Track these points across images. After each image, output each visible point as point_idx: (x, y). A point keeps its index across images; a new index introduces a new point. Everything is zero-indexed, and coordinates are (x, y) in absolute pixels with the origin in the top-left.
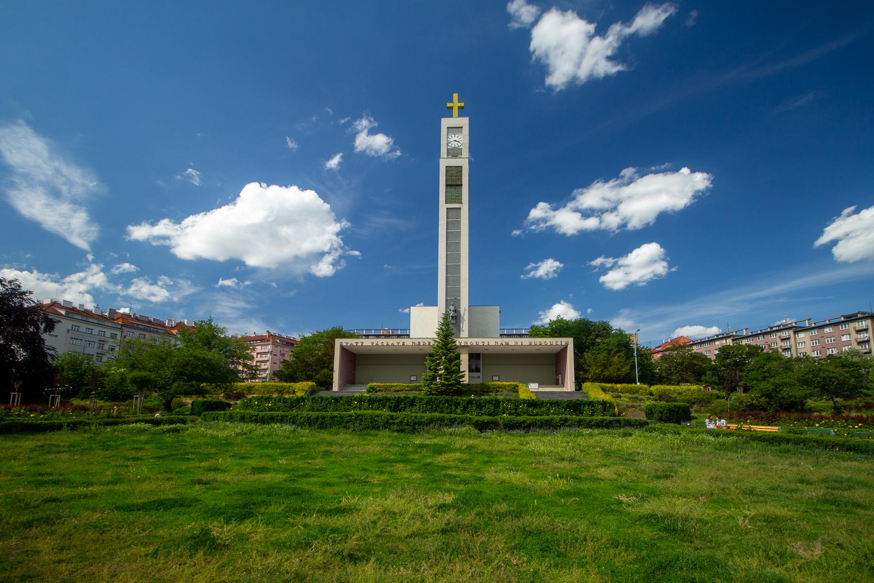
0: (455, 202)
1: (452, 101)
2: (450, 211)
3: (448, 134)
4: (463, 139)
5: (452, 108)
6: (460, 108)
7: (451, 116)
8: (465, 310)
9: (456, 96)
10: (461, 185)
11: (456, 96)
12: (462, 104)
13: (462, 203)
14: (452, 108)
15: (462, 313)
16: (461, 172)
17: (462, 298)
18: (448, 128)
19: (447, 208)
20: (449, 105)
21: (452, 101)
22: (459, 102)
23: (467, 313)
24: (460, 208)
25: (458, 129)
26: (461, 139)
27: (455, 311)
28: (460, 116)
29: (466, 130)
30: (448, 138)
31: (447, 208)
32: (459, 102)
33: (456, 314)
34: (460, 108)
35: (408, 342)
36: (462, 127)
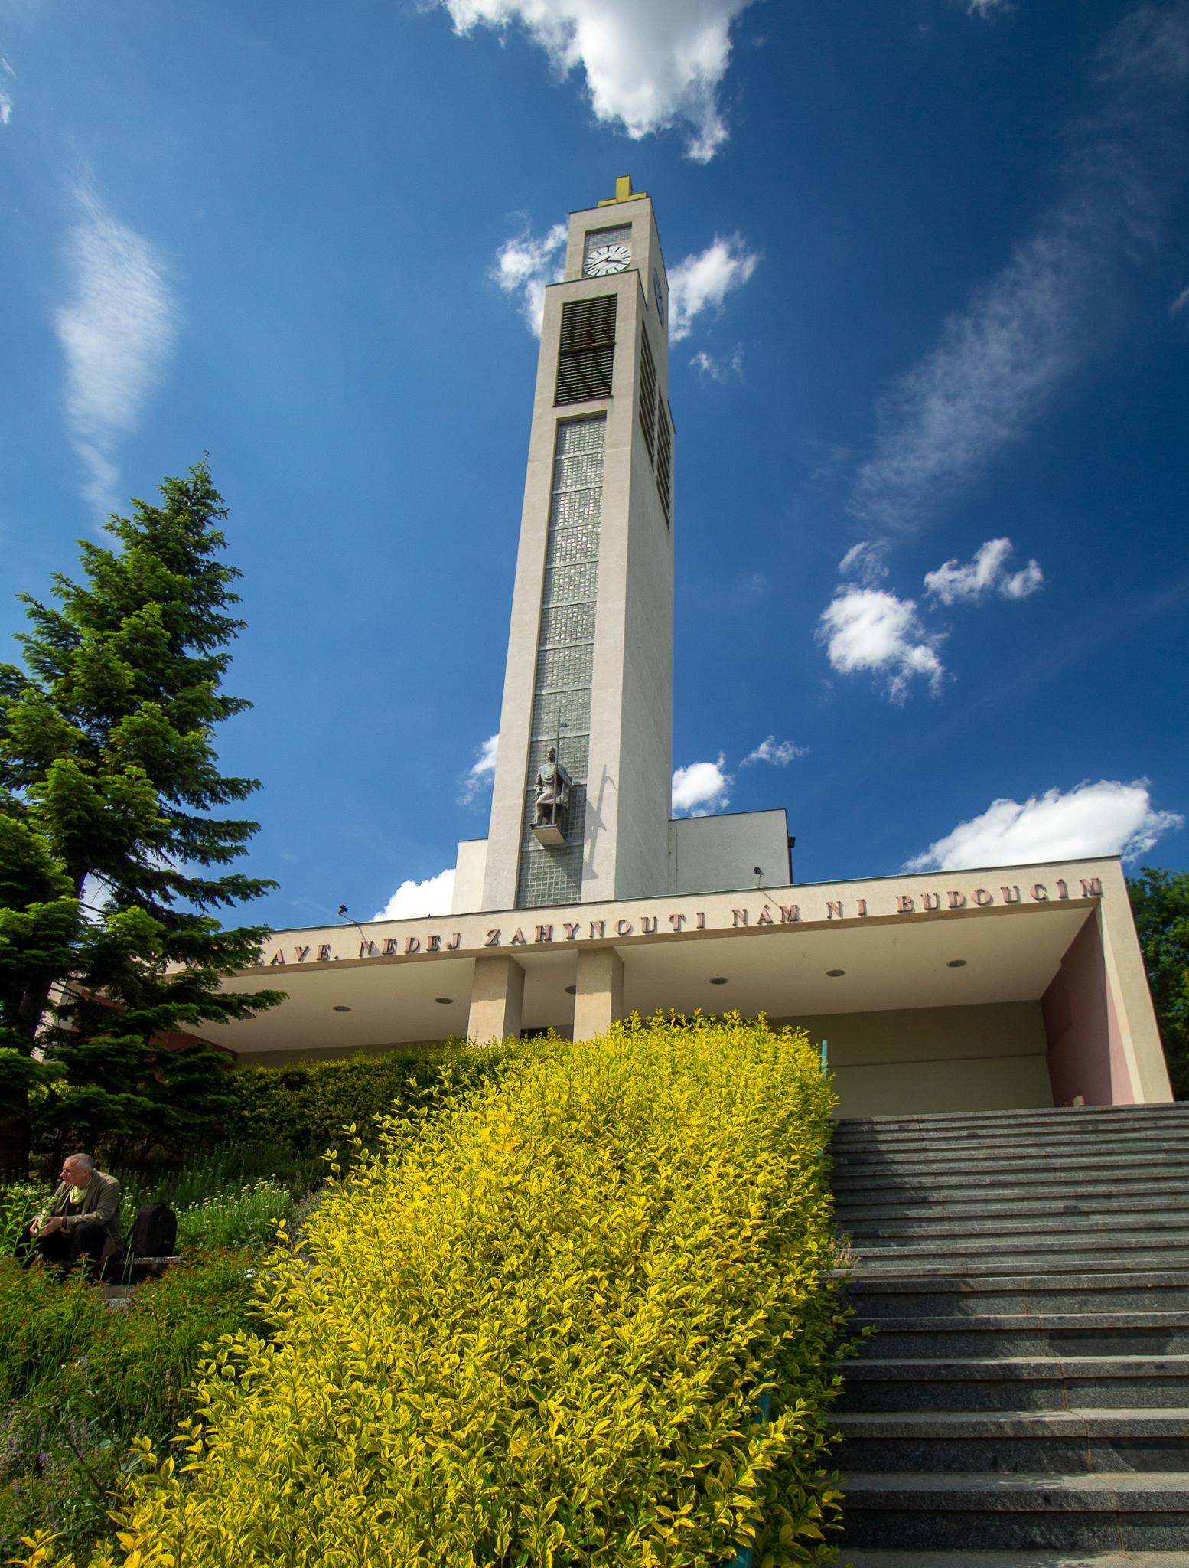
0: (590, 398)
2: (572, 433)
3: (586, 250)
4: (633, 252)
8: (605, 779)
13: (612, 397)
15: (592, 795)
17: (594, 730)
18: (589, 233)
23: (612, 793)
26: (629, 253)
27: (559, 780)
30: (585, 257)
31: (563, 424)
33: (562, 799)
36: (628, 226)
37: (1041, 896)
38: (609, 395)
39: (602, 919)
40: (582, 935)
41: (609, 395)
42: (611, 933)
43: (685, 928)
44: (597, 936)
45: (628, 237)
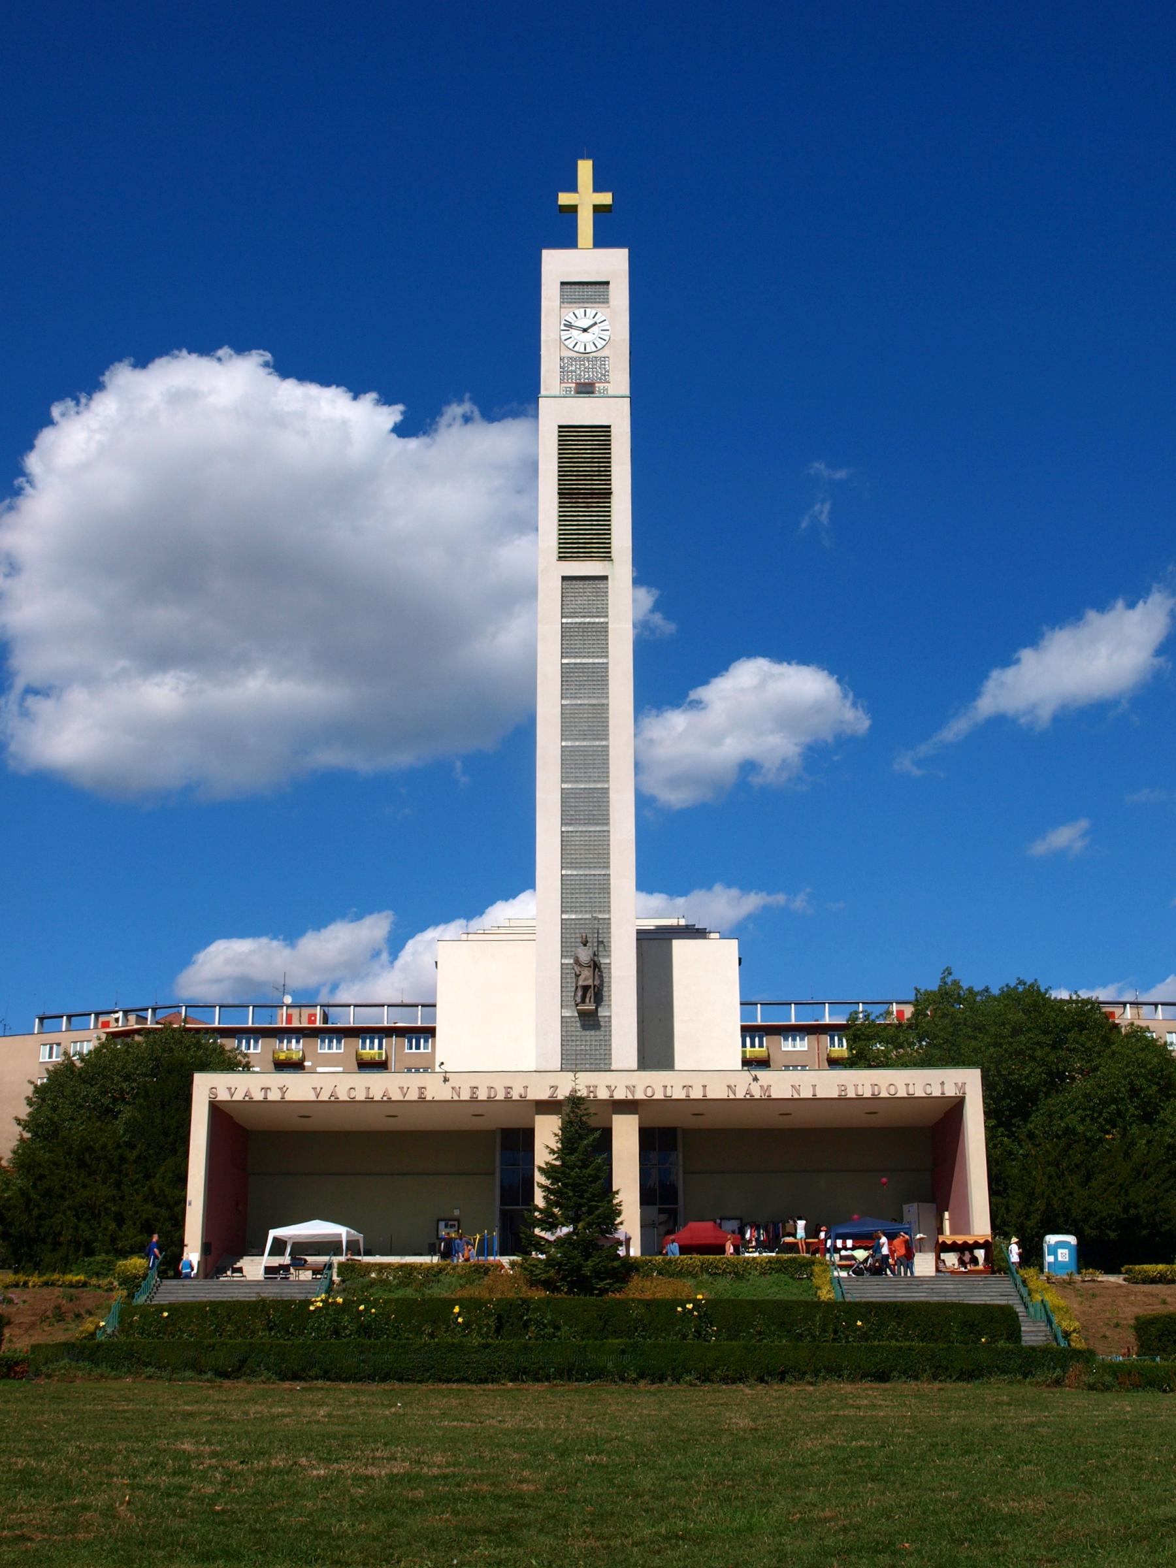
0: (589, 556)
1: (573, 187)
5: (573, 209)
6: (597, 209)
7: (569, 241)
9: (585, 169)
10: (607, 494)
11: (585, 169)
12: (606, 198)
13: (612, 560)
14: (573, 209)
16: (606, 445)
18: (563, 283)
19: (564, 578)
20: (564, 199)
21: (573, 187)
22: (598, 188)
24: (605, 578)
25: (602, 288)
28: (602, 240)
29: (620, 294)
32: (598, 188)
34: (597, 209)
35: (437, 1091)
36: (607, 283)
37: (929, 1092)
38: (607, 556)
39: (634, 1084)
40: (620, 1095)
41: (607, 556)
42: (640, 1095)
43: (692, 1096)
44: (630, 1097)
45: (605, 301)
